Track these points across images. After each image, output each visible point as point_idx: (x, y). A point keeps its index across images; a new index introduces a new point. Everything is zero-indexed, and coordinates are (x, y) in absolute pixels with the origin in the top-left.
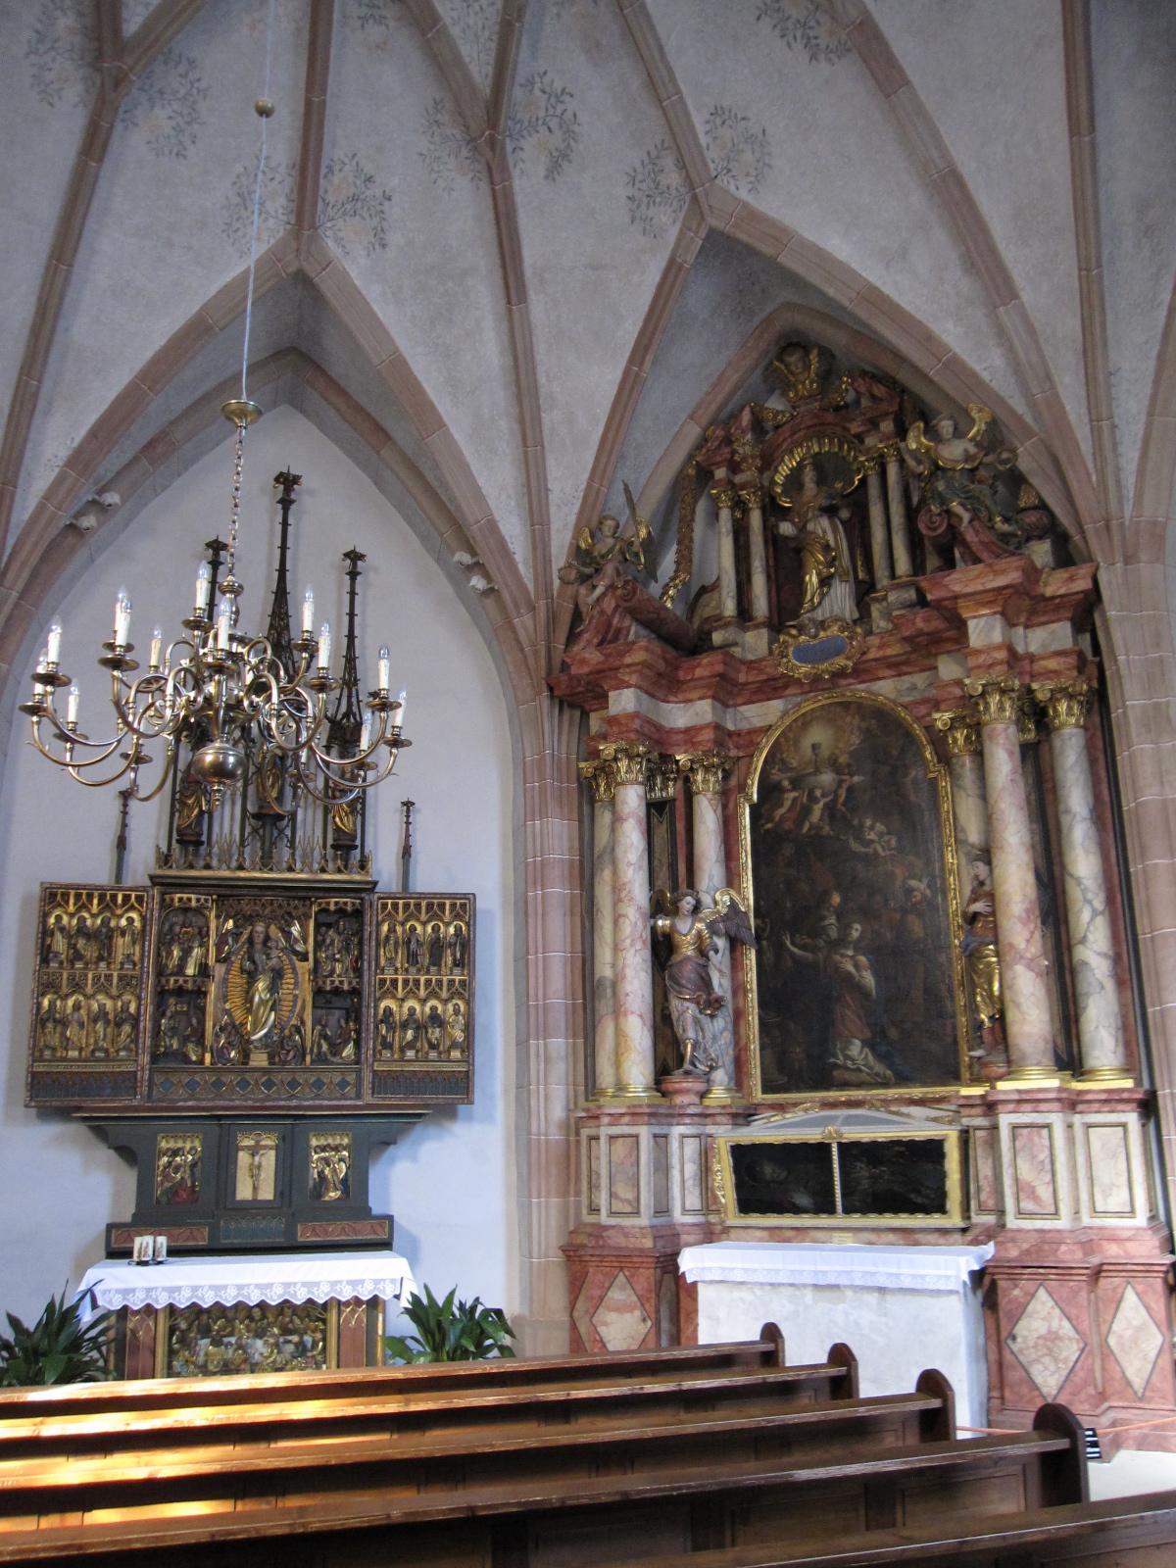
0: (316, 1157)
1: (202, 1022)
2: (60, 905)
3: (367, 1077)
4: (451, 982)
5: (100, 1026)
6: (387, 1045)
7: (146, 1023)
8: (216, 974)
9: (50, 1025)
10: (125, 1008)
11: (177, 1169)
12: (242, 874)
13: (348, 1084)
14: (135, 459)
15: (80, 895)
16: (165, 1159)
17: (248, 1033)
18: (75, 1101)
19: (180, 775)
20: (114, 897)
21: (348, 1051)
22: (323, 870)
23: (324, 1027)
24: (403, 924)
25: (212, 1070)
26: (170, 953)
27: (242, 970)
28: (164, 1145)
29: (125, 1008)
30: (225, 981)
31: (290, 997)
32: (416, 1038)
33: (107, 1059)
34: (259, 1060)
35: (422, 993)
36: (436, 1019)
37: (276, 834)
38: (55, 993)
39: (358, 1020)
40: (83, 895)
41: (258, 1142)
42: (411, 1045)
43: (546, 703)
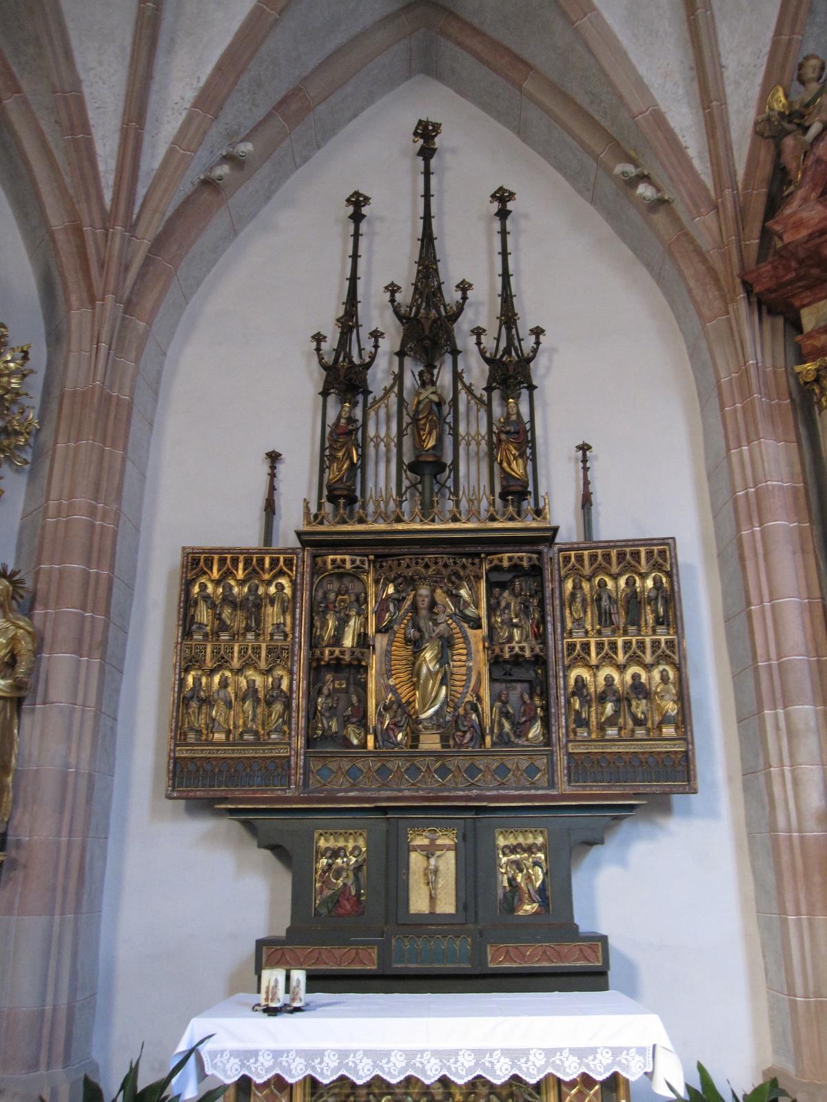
0: (504, 860)
1: (363, 701)
3: (561, 761)
4: (656, 644)
5: (248, 705)
6: (583, 723)
7: (299, 701)
8: (378, 646)
9: (194, 704)
11: (338, 874)
12: (400, 527)
13: (538, 770)
14: (269, 116)
15: (225, 559)
16: (324, 861)
17: (416, 712)
18: (219, 791)
19: (328, 430)
20: (261, 561)
21: (535, 731)
22: (492, 519)
23: (505, 703)
24: (589, 580)
25: (376, 754)
26: (324, 624)
27: (407, 641)
28: (322, 843)
30: (388, 653)
31: (463, 670)
32: (617, 712)
33: (258, 742)
34: (430, 742)
35: (621, 658)
36: (639, 689)
37: (436, 488)
38: (200, 668)
39: (545, 694)
40: (228, 559)
41: (433, 841)
43: (743, 307)
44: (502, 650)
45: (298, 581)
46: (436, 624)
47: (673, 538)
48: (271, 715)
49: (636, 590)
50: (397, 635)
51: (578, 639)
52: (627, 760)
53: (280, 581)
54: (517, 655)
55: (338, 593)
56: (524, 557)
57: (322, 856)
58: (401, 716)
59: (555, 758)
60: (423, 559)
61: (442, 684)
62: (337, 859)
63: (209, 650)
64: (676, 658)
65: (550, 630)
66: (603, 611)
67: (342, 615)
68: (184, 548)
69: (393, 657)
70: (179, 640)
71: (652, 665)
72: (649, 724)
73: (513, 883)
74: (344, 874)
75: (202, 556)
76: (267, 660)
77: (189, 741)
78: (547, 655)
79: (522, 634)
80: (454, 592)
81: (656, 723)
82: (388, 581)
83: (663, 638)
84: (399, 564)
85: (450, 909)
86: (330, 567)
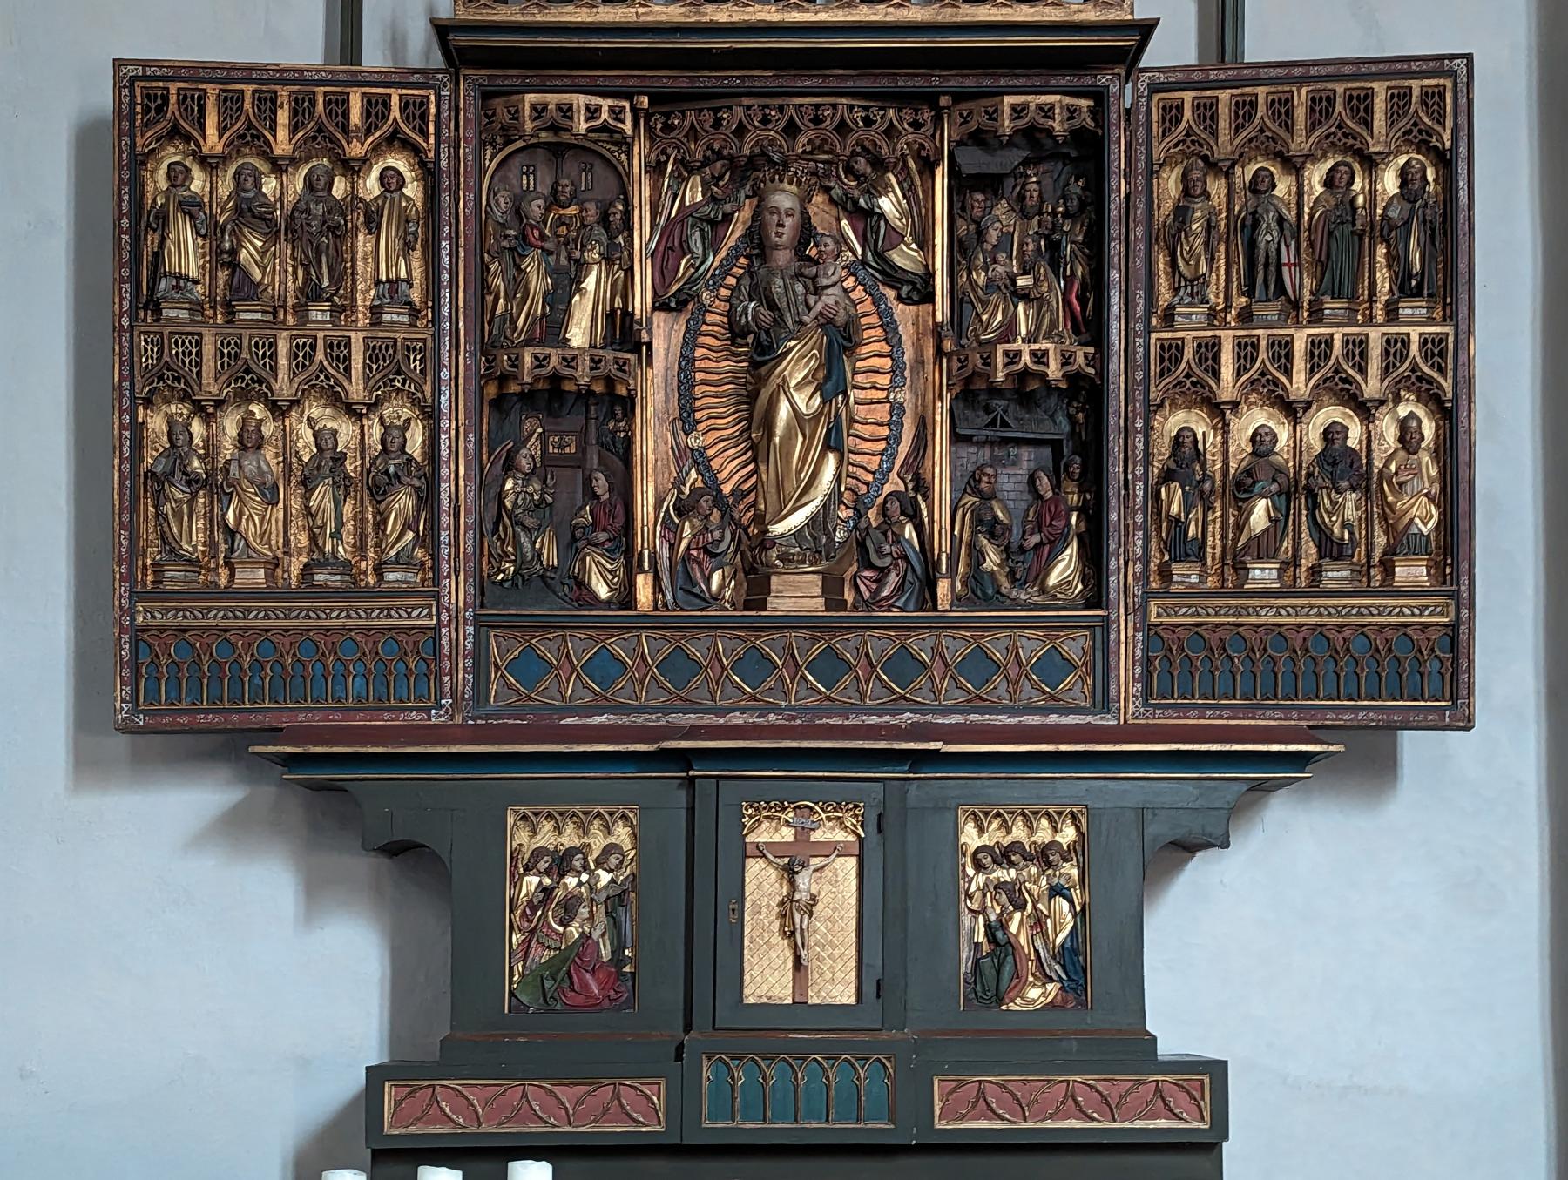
2: (175, 133)
4: (1395, 349)
5: (322, 497)
6: (1182, 547)
8: (659, 346)
9: (178, 493)
10: (393, 438)
11: (568, 909)
16: (531, 881)
20: (339, 106)
23: (987, 498)
25: (654, 623)
26: (518, 283)
27: (735, 332)
29: (393, 438)
30: (686, 362)
31: (882, 412)
33: (352, 591)
34: (797, 594)
35: (1299, 384)
38: (185, 397)
39: (1093, 478)
41: (802, 833)
42: (1264, 547)
44: (989, 361)
45: (444, 163)
46: (818, 291)
47: (1469, 58)
48: (385, 522)
49: (1354, 199)
50: (710, 317)
51: (1190, 330)
52: (1298, 644)
53: (391, 162)
54: (1026, 372)
55: (554, 200)
56: (1058, 107)
57: (527, 869)
58: (722, 528)
59: (1112, 637)
60: (781, 109)
61: (827, 447)
62: (562, 876)
63: (208, 349)
64: (1447, 384)
65: (1115, 309)
66: (1261, 258)
67: (564, 261)
68: (118, 63)
69: (699, 376)
70: (125, 321)
71: (1383, 402)
72: (1360, 555)
73: (999, 934)
74: (584, 912)
75: (173, 88)
76: (367, 379)
77: (168, 586)
78: (1102, 372)
79: (1039, 321)
80: (862, 201)
81: (1378, 552)
82: (686, 168)
83: (1415, 333)
84: (717, 123)
85: (847, 996)
86: (529, 127)
